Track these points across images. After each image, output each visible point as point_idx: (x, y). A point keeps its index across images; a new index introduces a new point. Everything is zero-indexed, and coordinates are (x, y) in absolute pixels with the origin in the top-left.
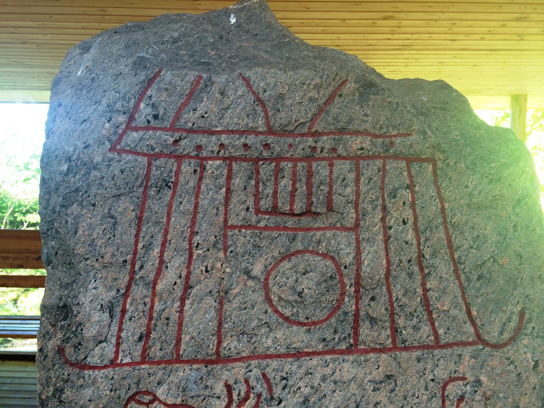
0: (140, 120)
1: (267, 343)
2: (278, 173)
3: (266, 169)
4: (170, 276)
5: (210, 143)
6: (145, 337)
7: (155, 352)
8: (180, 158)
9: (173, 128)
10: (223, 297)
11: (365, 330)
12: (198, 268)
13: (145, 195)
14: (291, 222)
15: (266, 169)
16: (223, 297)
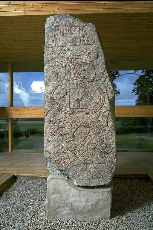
0: (55, 23)
1: (68, 44)
2: (69, 28)
3: (67, 28)
4: (58, 38)
5: (62, 25)
6: (56, 44)
7: (57, 46)
8: (59, 27)
9: (58, 24)
10: (63, 40)
11: (78, 43)
12: (61, 38)
13: (55, 30)
14: (70, 33)
15: (67, 28)
16: (63, 40)
